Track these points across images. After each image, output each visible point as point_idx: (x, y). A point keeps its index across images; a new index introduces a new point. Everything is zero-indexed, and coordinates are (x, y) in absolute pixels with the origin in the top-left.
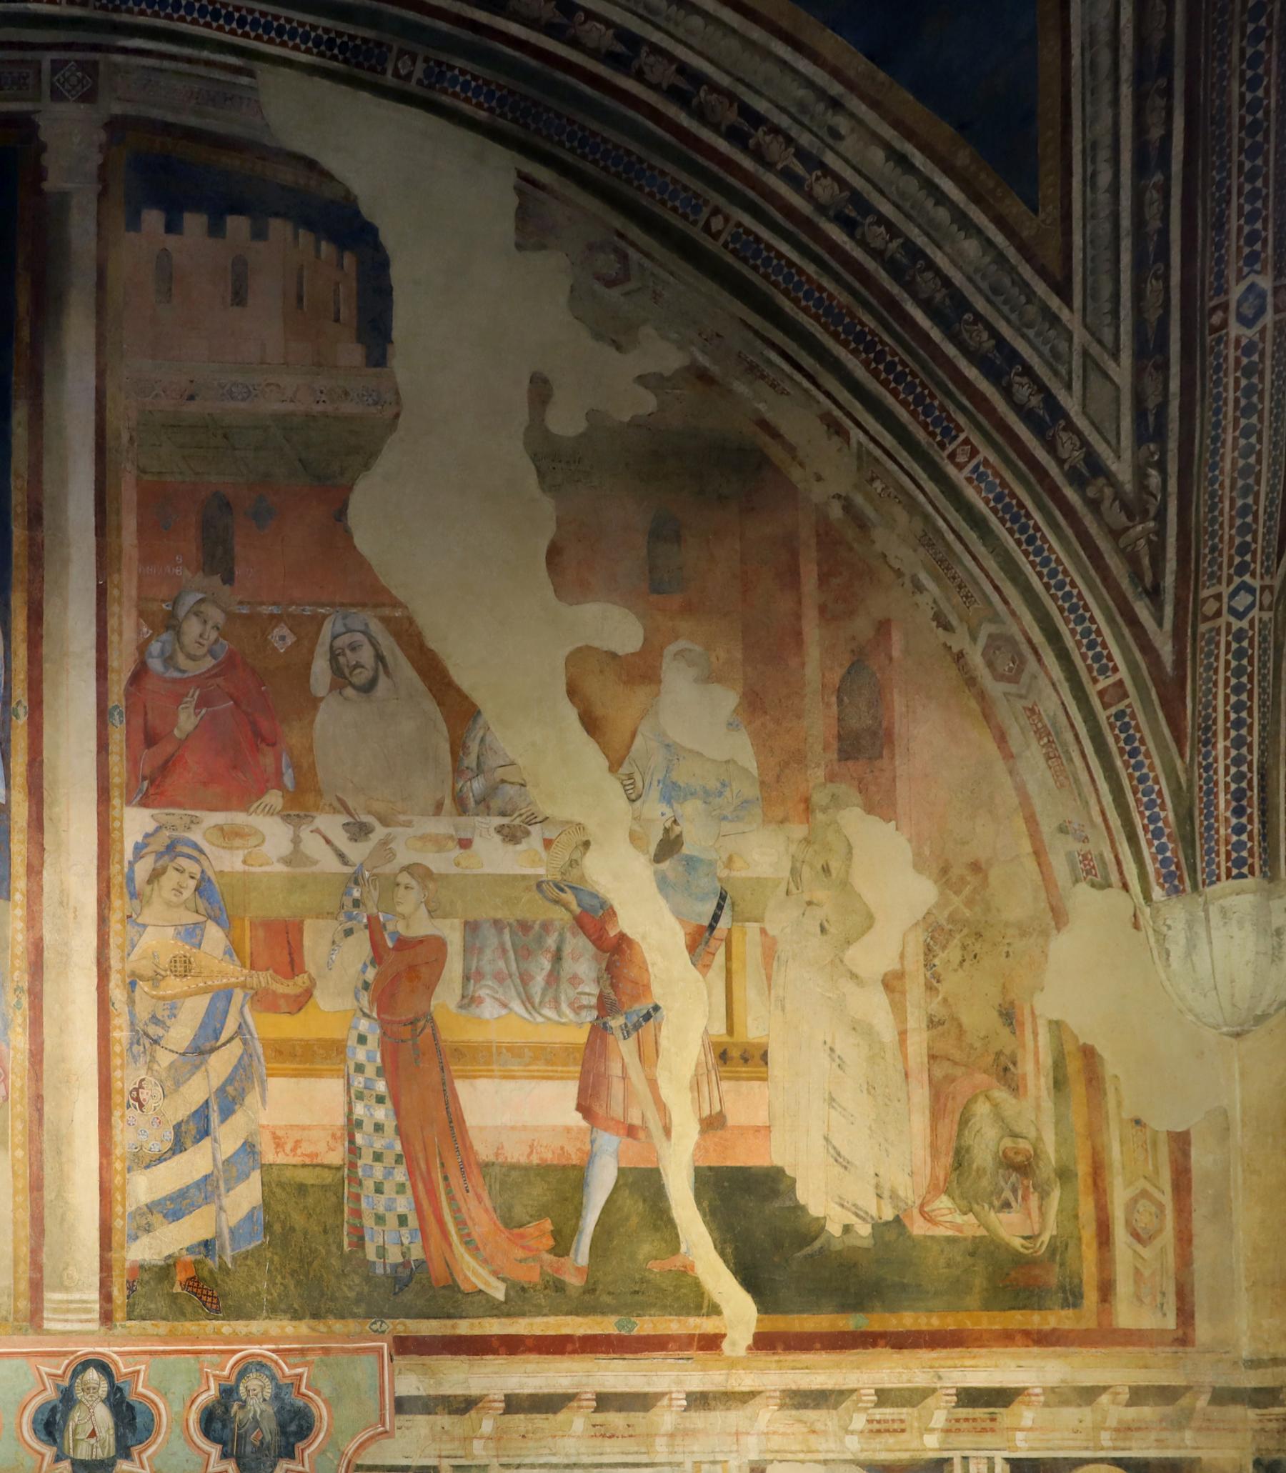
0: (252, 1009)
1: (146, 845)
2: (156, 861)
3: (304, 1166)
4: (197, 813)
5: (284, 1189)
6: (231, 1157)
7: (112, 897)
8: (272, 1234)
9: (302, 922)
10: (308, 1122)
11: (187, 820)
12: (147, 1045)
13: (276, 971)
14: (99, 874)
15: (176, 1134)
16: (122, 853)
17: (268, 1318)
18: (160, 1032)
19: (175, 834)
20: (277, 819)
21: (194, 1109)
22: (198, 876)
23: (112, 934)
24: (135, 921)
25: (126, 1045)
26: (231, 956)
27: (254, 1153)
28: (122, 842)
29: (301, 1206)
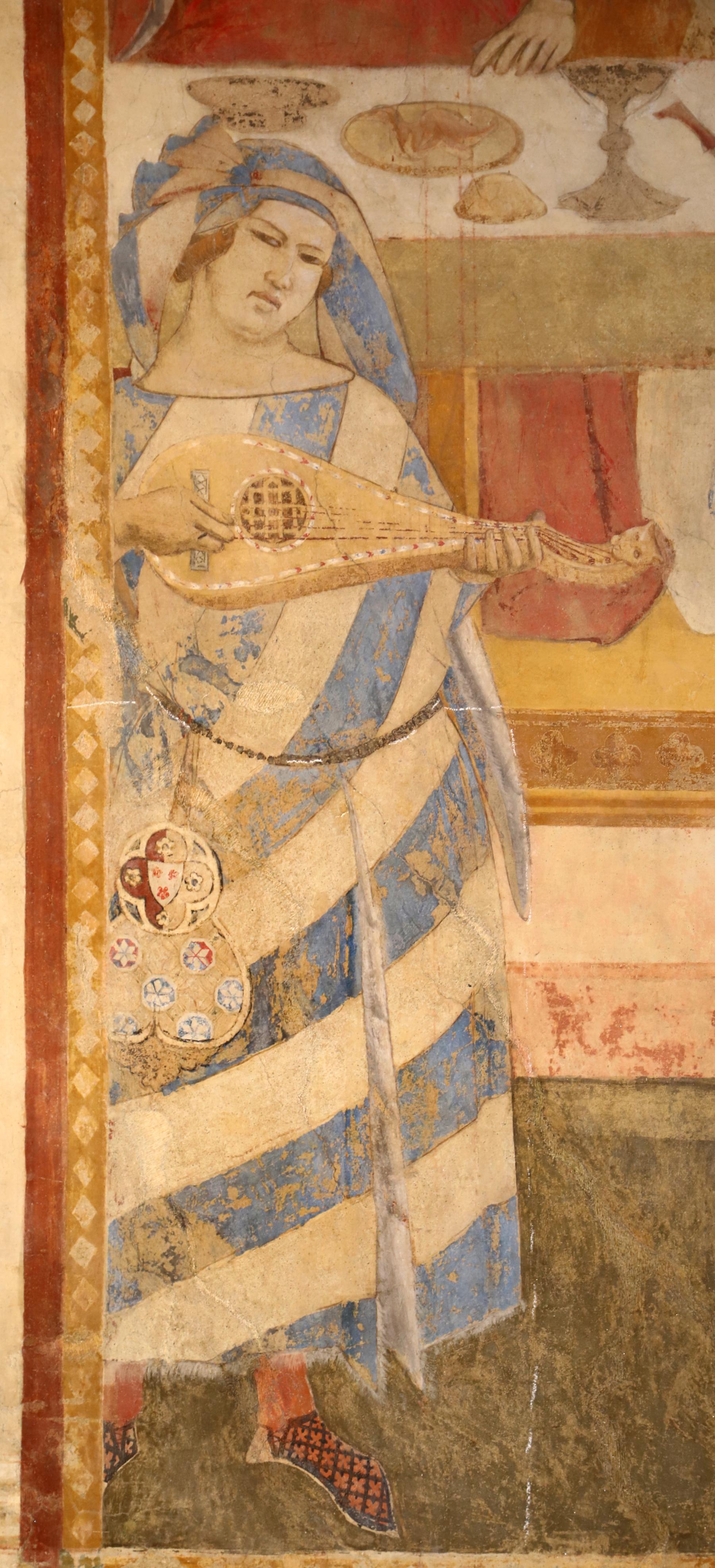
0: (484, 628)
1: (173, 170)
2: (201, 216)
3: (642, 1084)
4: (323, 75)
5: (584, 1154)
6: (423, 1056)
7: (72, 317)
8: (547, 1287)
9: (632, 379)
10: (653, 956)
11: (292, 96)
12: (174, 736)
13: (554, 521)
14: (31, 255)
15: (257, 992)
16: (99, 193)
17: (539, 1545)
18: (212, 697)
19: (255, 135)
20: (560, 83)
21: (310, 917)
22: (326, 256)
23: (69, 423)
24: (138, 385)
25: (109, 735)
26: (422, 480)
27: (490, 1045)
28: (100, 163)
29: (634, 1205)
